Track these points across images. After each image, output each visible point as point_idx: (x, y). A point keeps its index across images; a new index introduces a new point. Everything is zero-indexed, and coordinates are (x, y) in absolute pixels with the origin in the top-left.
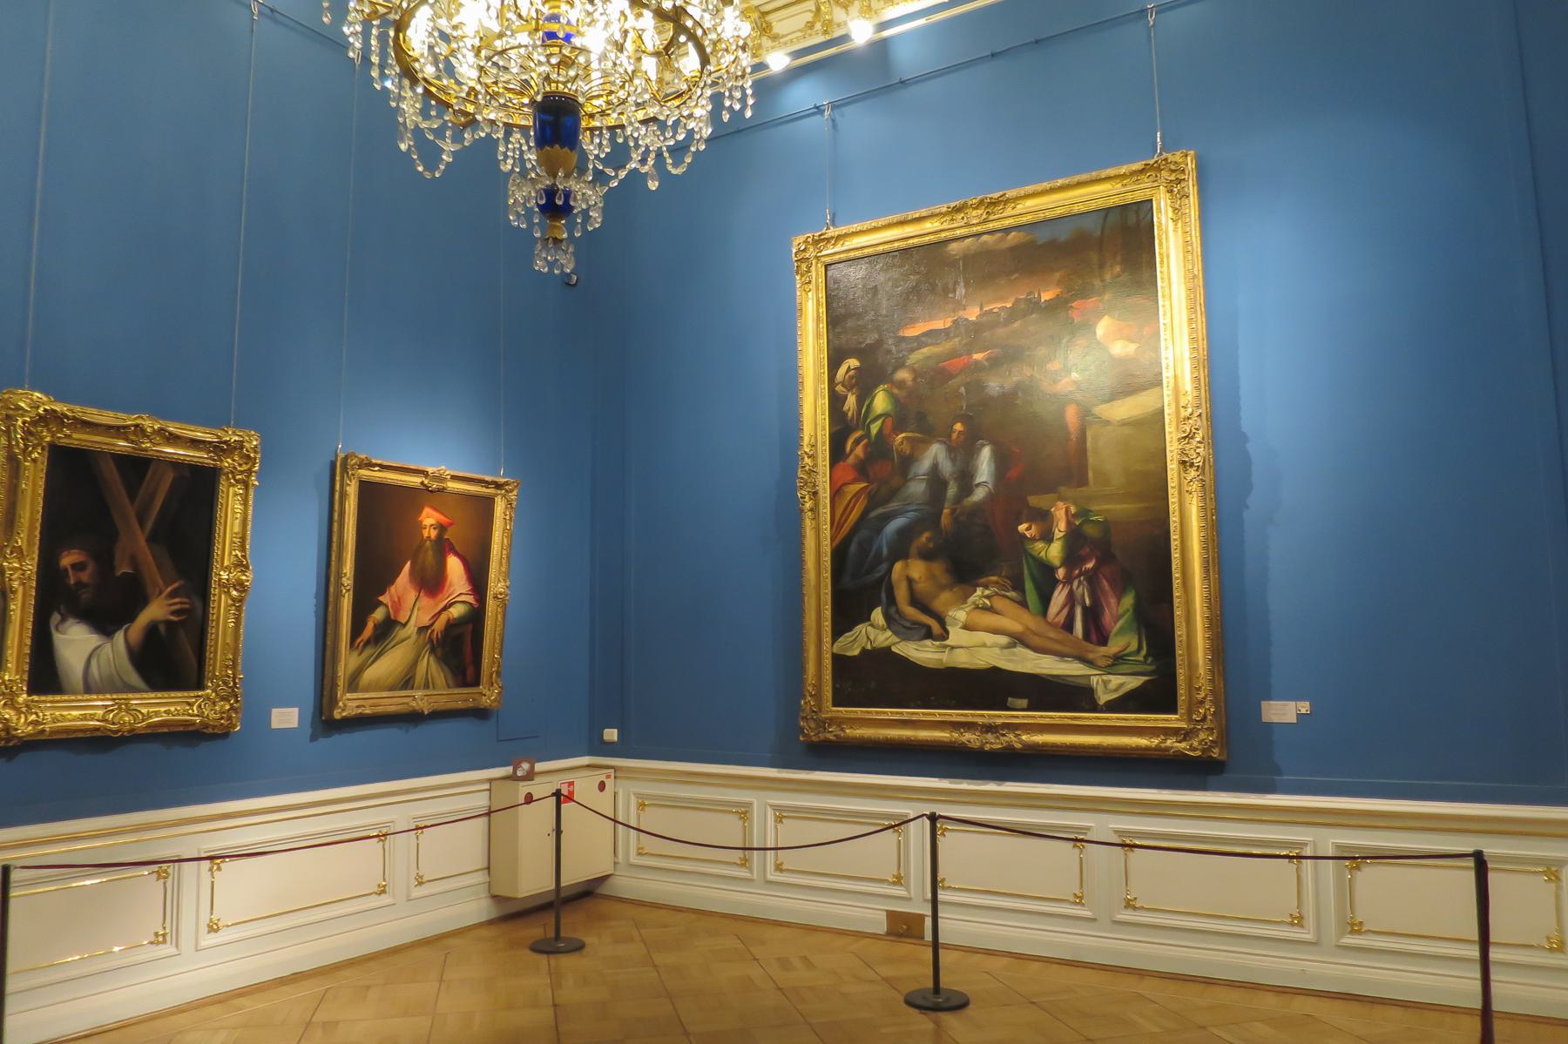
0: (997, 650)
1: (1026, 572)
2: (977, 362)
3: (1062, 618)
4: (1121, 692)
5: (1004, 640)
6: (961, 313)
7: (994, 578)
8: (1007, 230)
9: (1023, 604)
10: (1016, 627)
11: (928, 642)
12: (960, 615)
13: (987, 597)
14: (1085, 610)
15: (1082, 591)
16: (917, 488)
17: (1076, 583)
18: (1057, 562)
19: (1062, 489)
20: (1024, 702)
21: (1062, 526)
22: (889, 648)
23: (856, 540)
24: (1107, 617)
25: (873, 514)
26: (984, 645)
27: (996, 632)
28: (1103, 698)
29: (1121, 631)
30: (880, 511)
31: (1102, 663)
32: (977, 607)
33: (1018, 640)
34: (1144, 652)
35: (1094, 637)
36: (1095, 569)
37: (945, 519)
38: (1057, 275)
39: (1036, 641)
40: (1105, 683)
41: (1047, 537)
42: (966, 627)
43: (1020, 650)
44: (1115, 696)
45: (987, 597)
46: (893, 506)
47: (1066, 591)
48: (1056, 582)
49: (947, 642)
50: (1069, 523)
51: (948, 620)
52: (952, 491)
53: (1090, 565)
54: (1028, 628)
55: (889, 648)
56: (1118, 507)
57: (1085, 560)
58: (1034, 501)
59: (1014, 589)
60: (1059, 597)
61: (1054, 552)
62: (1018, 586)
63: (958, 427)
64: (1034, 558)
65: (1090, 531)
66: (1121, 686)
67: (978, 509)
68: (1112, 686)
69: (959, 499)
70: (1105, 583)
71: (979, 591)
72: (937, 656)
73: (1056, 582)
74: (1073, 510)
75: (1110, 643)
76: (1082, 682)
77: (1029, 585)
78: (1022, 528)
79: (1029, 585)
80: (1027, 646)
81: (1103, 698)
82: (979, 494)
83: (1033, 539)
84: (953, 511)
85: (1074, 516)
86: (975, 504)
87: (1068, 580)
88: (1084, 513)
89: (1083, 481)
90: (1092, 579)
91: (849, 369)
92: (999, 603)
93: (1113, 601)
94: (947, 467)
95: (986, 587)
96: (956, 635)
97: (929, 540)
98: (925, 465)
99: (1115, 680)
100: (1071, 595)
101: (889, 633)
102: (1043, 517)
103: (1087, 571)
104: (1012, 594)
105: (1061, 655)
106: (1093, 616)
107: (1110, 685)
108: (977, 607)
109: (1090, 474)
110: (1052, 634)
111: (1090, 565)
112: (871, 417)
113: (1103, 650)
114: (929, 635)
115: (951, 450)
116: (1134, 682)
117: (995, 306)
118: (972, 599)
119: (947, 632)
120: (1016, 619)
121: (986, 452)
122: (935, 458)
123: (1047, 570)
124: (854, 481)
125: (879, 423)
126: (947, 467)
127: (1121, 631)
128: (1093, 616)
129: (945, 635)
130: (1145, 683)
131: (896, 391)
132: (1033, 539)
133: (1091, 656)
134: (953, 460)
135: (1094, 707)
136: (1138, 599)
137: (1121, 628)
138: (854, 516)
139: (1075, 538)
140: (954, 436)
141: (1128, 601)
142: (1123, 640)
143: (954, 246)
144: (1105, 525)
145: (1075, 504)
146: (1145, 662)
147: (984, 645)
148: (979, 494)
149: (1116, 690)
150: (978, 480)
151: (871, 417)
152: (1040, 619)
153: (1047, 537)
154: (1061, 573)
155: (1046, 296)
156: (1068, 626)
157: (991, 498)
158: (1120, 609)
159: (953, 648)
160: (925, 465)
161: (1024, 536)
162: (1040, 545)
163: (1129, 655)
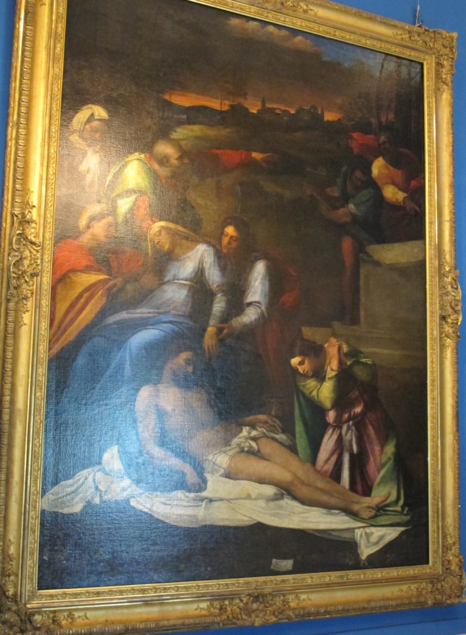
0: (262, 503)
1: (297, 412)
2: (254, 160)
3: (330, 466)
4: (381, 545)
5: (270, 490)
6: (242, 100)
7: (262, 417)
8: (295, 32)
9: (293, 449)
10: (284, 476)
11: (180, 494)
12: (223, 460)
13: (254, 439)
14: (352, 455)
15: (350, 436)
16: (176, 294)
17: (345, 428)
18: (328, 403)
19: (336, 324)
20: (288, 564)
21: (334, 364)
22: (127, 501)
23: (85, 350)
24: (371, 467)
25: (111, 319)
26: (249, 497)
27: (261, 481)
28: (365, 552)
29: (384, 481)
30: (124, 315)
31: (366, 514)
32: (242, 451)
33: (286, 490)
34: (401, 502)
35: (359, 488)
36: (363, 414)
37: (209, 339)
38: (339, 101)
39: (304, 491)
40: (368, 535)
41: (319, 375)
42: (228, 475)
43: (288, 502)
44: (376, 549)
45: (254, 439)
46: (142, 312)
47: (335, 437)
48: (326, 425)
49: (204, 494)
50: (341, 363)
51: (206, 465)
52: (219, 305)
53: (358, 410)
54: (295, 476)
55: (127, 501)
56: (385, 351)
57: (352, 405)
58: (307, 332)
59: (284, 432)
60: (328, 443)
61: (325, 392)
62: (288, 429)
63: (230, 230)
64: (304, 395)
65: (361, 374)
66: (382, 537)
67: (250, 332)
68: (373, 539)
69: (226, 318)
70: (370, 427)
71: (245, 431)
72: (190, 512)
73: (326, 425)
74: (345, 348)
75: (374, 493)
76: (347, 535)
77: (299, 428)
78: (295, 361)
79: (299, 428)
80: (295, 498)
81: (365, 552)
82: (250, 316)
83: (305, 376)
84: (220, 331)
85: (346, 355)
86: (245, 326)
87: (338, 424)
88: (354, 354)
89: (355, 321)
90: (359, 424)
91: (91, 118)
92: (268, 448)
93: (377, 448)
94: (214, 277)
95: (253, 426)
96: (216, 485)
97: (188, 362)
98: (186, 268)
99: (377, 532)
100: (340, 440)
101: (127, 482)
102: (315, 351)
103: (356, 416)
104: (281, 437)
105: (328, 507)
106: (359, 463)
107: (373, 538)
108: (242, 451)
109: (362, 313)
110: (320, 484)
111: (358, 410)
112: (118, 191)
113: (367, 501)
114: (182, 485)
115: (220, 256)
116: (392, 534)
117: (278, 107)
118: (236, 441)
119: (205, 481)
120: (284, 467)
121: (260, 268)
122: (201, 262)
123: (318, 410)
124: (88, 269)
125: (132, 198)
126: (214, 277)
127: (384, 481)
128: (359, 463)
129: (201, 485)
130: (402, 533)
131: (156, 167)
132: (305, 376)
133: (356, 507)
134: (223, 269)
135: (357, 565)
136: (398, 446)
137: (383, 477)
138: (88, 314)
139: (345, 378)
140: (225, 240)
141: (390, 449)
142: (385, 491)
143: (234, 22)
144: (373, 367)
145: (348, 344)
146: (401, 513)
147: (249, 497)
148: (250, 316)
149: (377, 543)
150: (250, 298)
151: (118, 191)
152: (308, 465)
153: (319, 375)
154: (331, 416)
155: (329, 116)
156: (336, 475)
157: (264, 320)
158: (383, 456)
159: (211, 501)
160: (186, 268)
161: (295, 371)
162: (312, 383)
163: (388, 505)
